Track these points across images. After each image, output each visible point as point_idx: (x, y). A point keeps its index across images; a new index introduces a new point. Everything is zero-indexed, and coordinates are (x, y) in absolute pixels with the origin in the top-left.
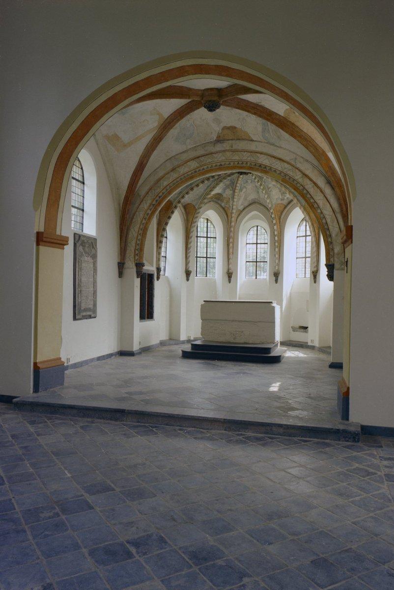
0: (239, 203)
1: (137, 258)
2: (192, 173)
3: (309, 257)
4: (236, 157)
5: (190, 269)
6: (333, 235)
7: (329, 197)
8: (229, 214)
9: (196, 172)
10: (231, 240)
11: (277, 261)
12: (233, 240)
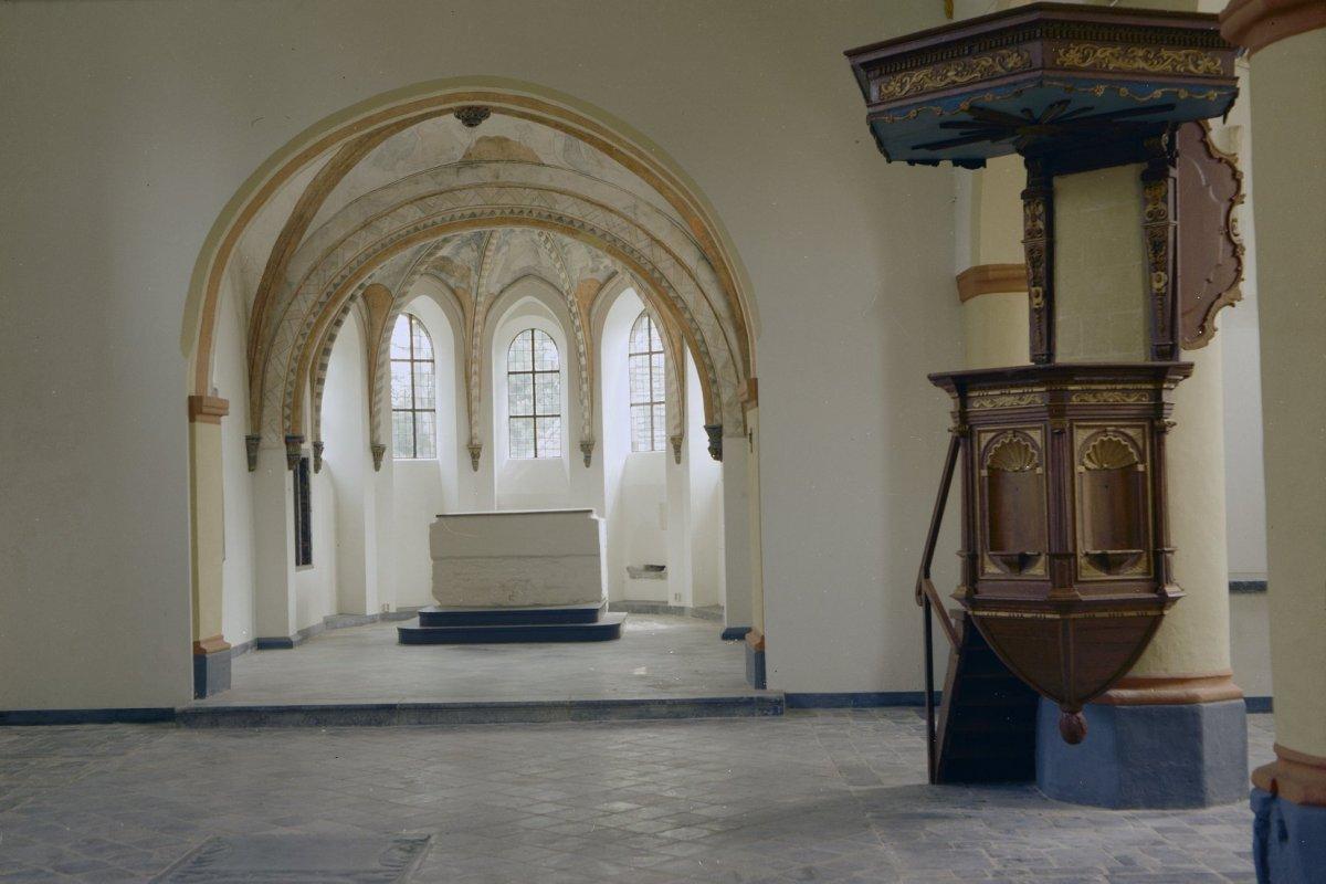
0: (491, 280)
3: (660, 403)
4: (507, 200)
5: (382, 442)
6: (719, 366)
7: (706, 287)
9: (416, 229)
10: (475, 367)
11: (587, 415)
12: (480, 369)
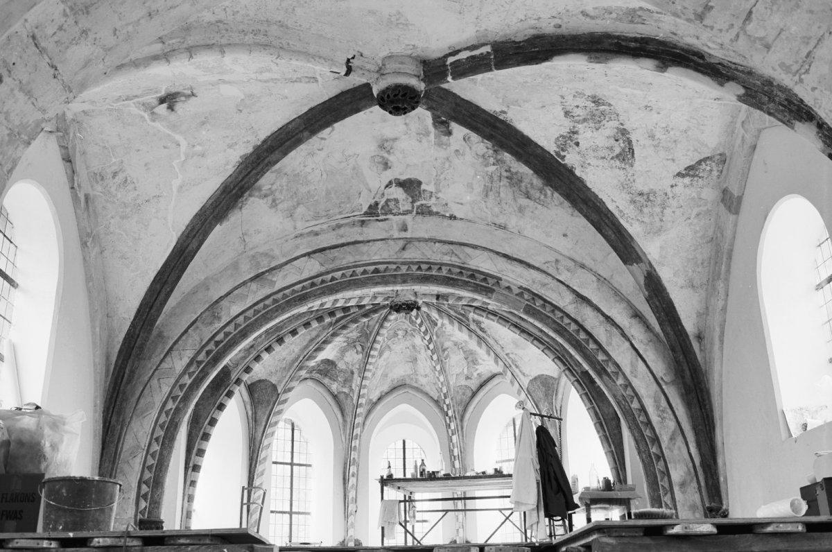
0: (374, 386)
1: (143, 504)
2: (304, 288)
8: (348, 410)
9: (313, 285)
10: (353, 469)
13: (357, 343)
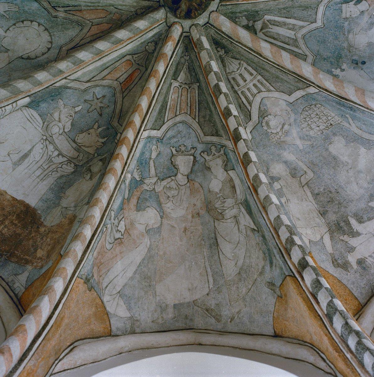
13: (95, 160)
